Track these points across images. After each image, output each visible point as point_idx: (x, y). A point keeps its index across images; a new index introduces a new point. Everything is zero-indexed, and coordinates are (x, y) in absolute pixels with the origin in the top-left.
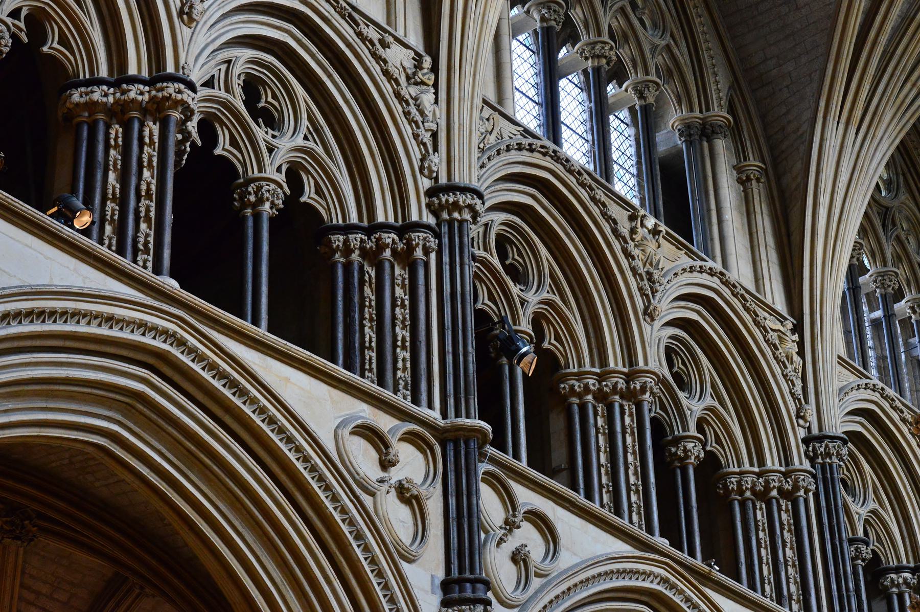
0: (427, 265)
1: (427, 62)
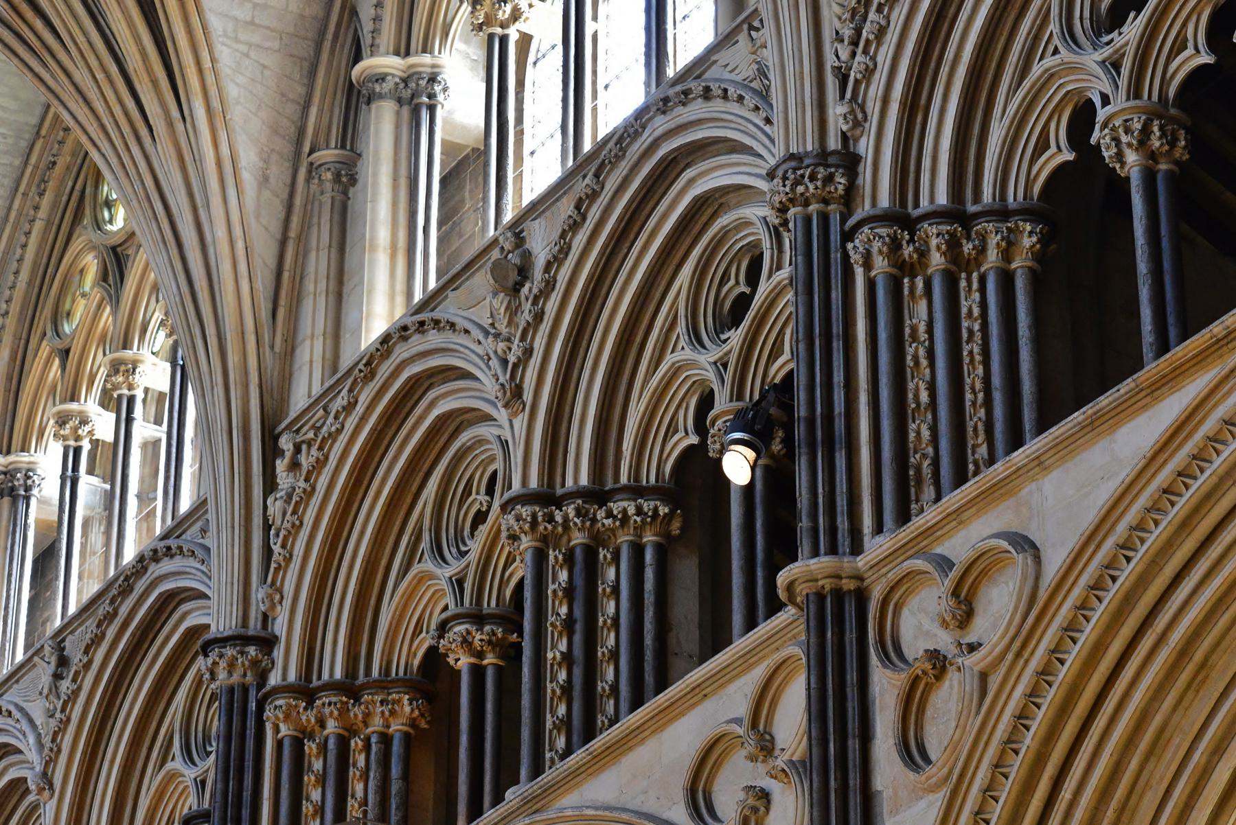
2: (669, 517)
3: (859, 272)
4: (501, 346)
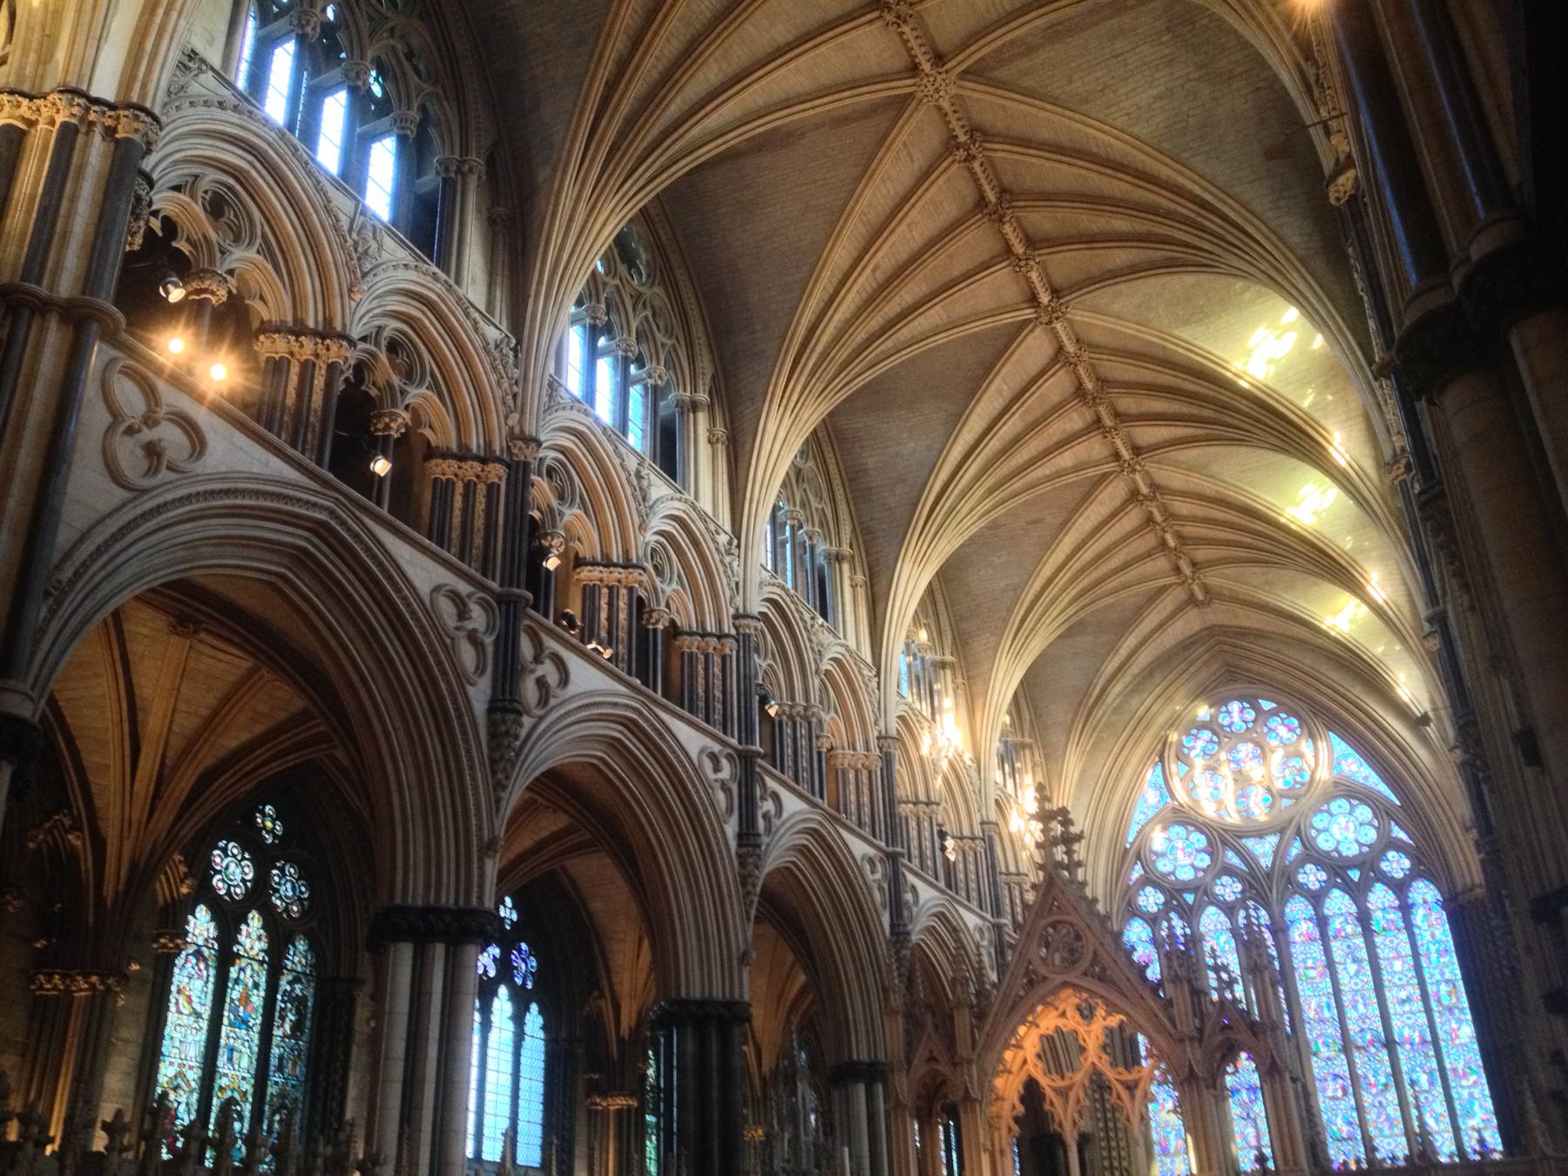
0: (731, 657)
1: (735, 541)
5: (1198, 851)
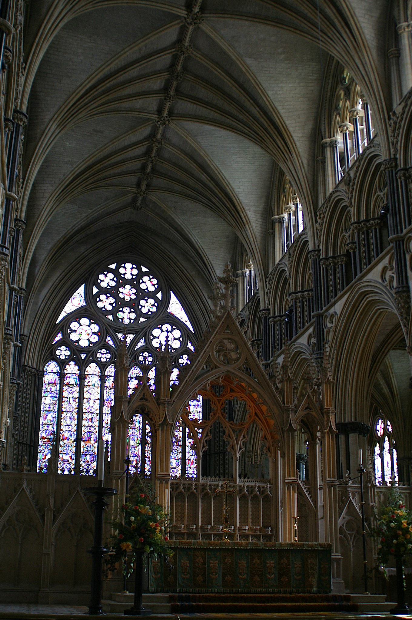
2: (381, 222)
3: (399, 180)
4: (347, 195)
5: (93, 333)
